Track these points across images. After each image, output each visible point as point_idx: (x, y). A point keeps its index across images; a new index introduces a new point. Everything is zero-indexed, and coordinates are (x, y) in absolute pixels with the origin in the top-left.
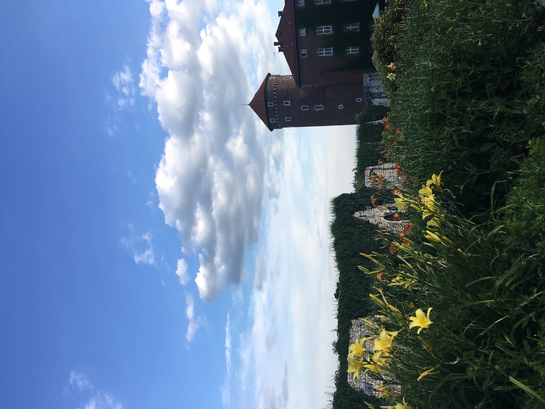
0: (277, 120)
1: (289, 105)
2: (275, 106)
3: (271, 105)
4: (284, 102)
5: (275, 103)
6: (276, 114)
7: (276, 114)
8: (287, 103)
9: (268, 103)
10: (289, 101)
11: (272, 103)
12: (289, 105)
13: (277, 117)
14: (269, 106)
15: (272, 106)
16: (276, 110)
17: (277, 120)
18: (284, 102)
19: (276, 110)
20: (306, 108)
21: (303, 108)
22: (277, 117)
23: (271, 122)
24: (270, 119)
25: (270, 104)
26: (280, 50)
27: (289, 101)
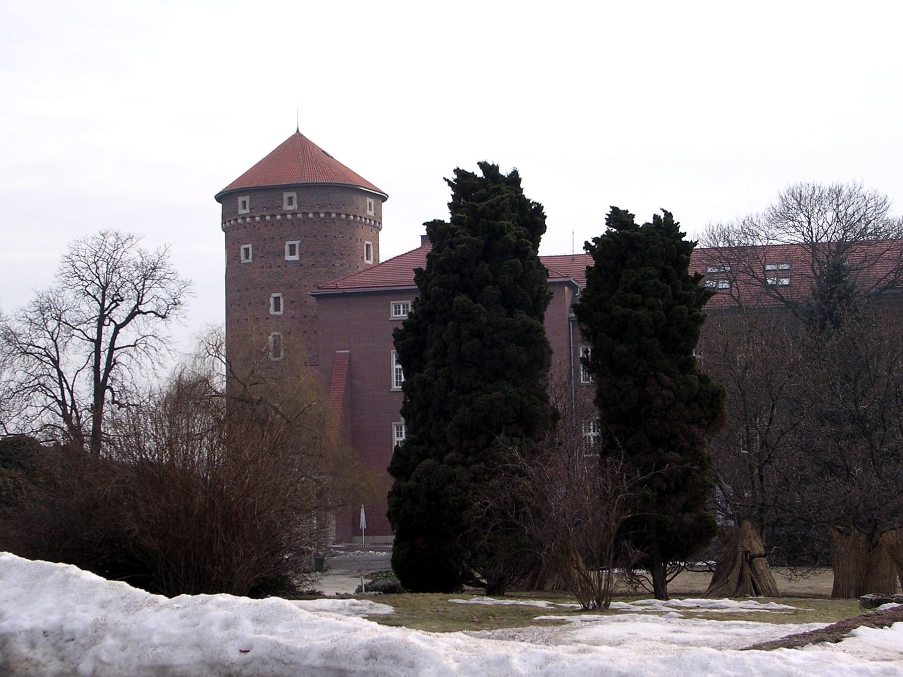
0: (244, 218)
1: (288, 258)
2: (284, 215)
3: (290, 205)
4: (297, 243)
5: (294, 214)
8: (292, 253)
9: (294, 195)
10: (296, 258)
11: (295, 206)
13: (253, 218)
14: (286, 195)
15: (287, 207)
20: (277, 308)
21: (277, 299)
22: (253, 218)
23: (240, 199)
24: (247, 198)
25: (291, 199)
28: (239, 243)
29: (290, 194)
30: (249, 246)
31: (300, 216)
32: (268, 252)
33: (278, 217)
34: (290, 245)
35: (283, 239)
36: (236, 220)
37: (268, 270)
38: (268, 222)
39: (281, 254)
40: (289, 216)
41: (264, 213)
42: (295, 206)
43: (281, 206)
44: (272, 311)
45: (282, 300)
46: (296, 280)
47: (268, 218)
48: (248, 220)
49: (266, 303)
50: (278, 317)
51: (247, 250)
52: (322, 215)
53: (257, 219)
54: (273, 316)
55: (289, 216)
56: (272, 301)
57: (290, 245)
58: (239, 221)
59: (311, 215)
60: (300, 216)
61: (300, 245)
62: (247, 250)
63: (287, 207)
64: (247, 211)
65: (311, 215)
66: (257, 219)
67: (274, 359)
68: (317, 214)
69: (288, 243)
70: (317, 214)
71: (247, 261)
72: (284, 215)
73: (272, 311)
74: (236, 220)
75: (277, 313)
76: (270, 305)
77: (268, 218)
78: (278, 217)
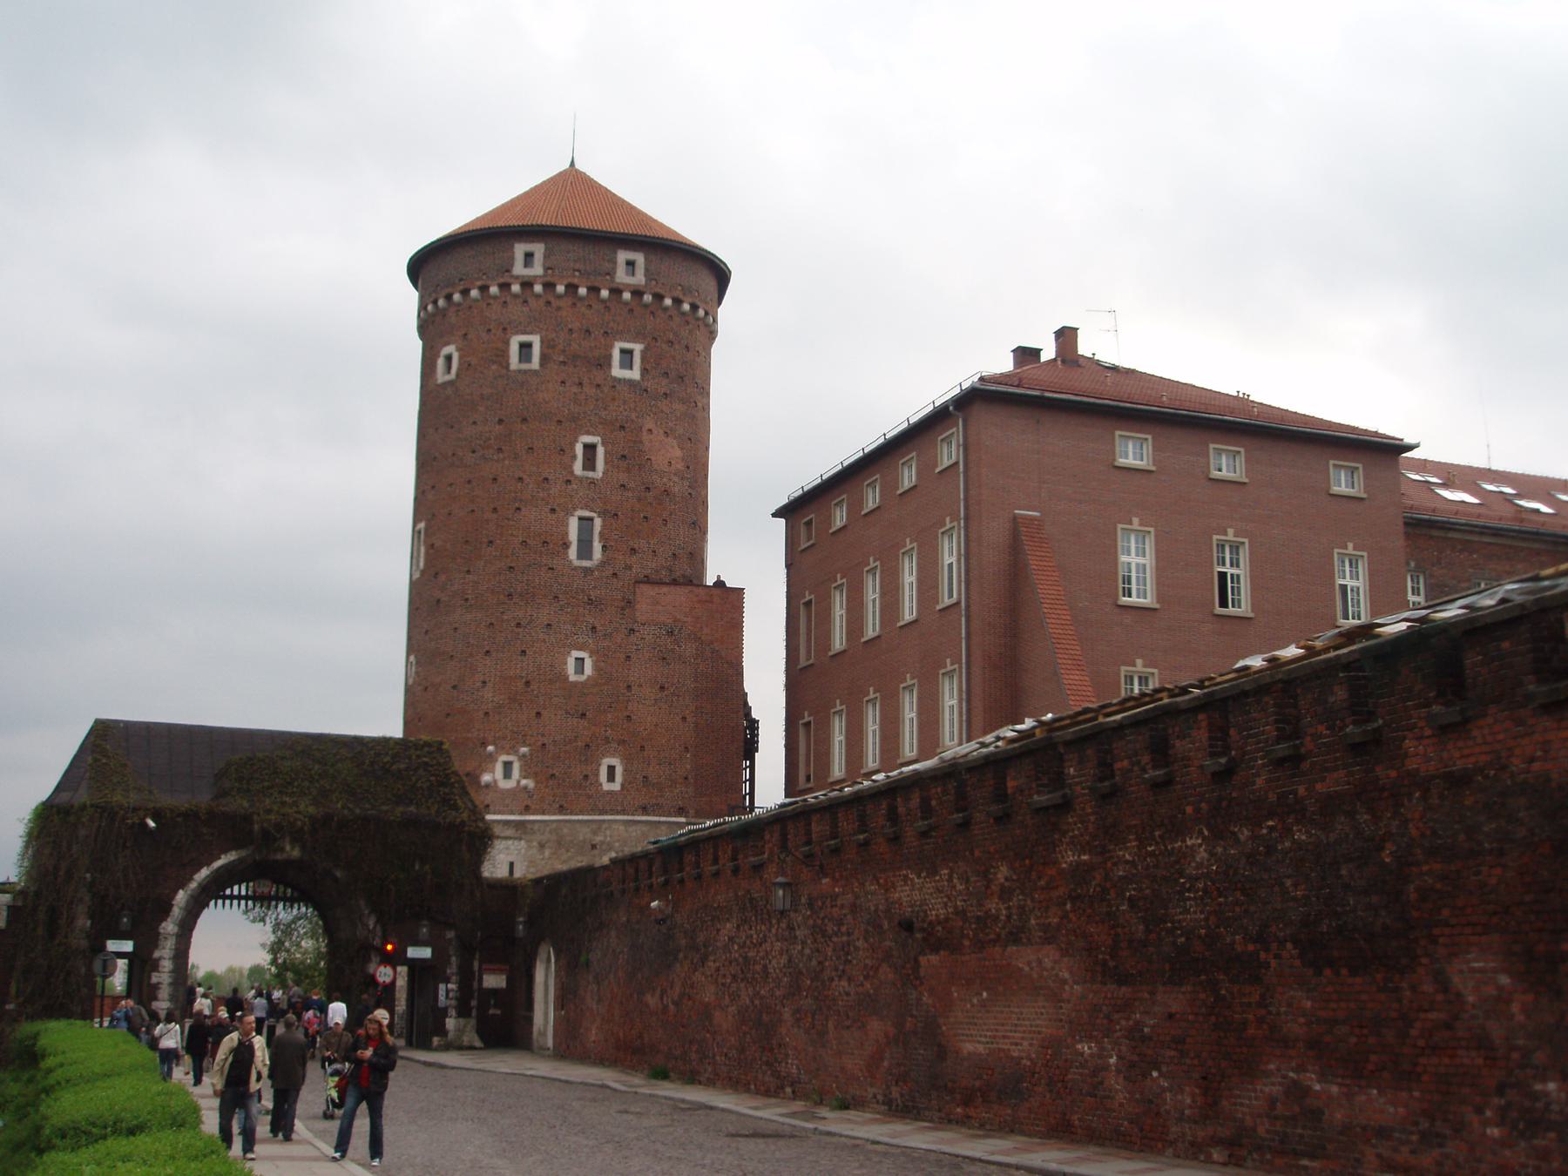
1: (617, 372)
4: (637, 348)
5: (637, 293)
6: (572, 288)
7: (572, 288)
9: (639, 258)
10: (635, 374)
11: (639, 278)
12: (617, 372)
13: (549, 286)
14: (623, 256)
15: (621, 276)
16: (594, 290)
17: (527, 284)
18: (637, 348)
19: (594, 290)
20: (590, 463)
21: (590, 449)
26: (1026, 355)
27: (635, 374)
28: (506, 330)
29: (631, 255)
30: (535, 340)
31: (648, 298)
32: (575, 357)
33: (605, 293)
34: (623, 351)
35: (610, 335)
36: (505, 287)
37: (575, 389)
38: (581, 299)
39: (605, 362)
40: (627, 296)
41: (576, 281)
42: (639, 278)
43: (611, 273)
44: (578, 468)
45: (600, 451)
46: (633, 416)
47: (582, 291)
48: (538, 288)
49: (565, 452)
50: (593, 482)
51: (525, 347)
52: (686, 307)
53: (560, 289)
54: (581, 479)
55: (627, 296)
56: (579, 449)
57: (623, 351)
58: (516, 288)
59: (668, 302)
60: (648, 298)
61: (643, 353)
62: (525, 347)
63: (621, 276)
64: (537, 270)
65: (668, 302)
66: (560, 289)
67: (577, 563)
68: (678, 302)
69: (619, 345)
70: (678, 302)
71: (525, 366)
72: (616, 291)
73: (578, 468)
74: (505, 287)
75: (590, 474)
76: (574, 457)
77: (582, 291)
78: (605, 293)
